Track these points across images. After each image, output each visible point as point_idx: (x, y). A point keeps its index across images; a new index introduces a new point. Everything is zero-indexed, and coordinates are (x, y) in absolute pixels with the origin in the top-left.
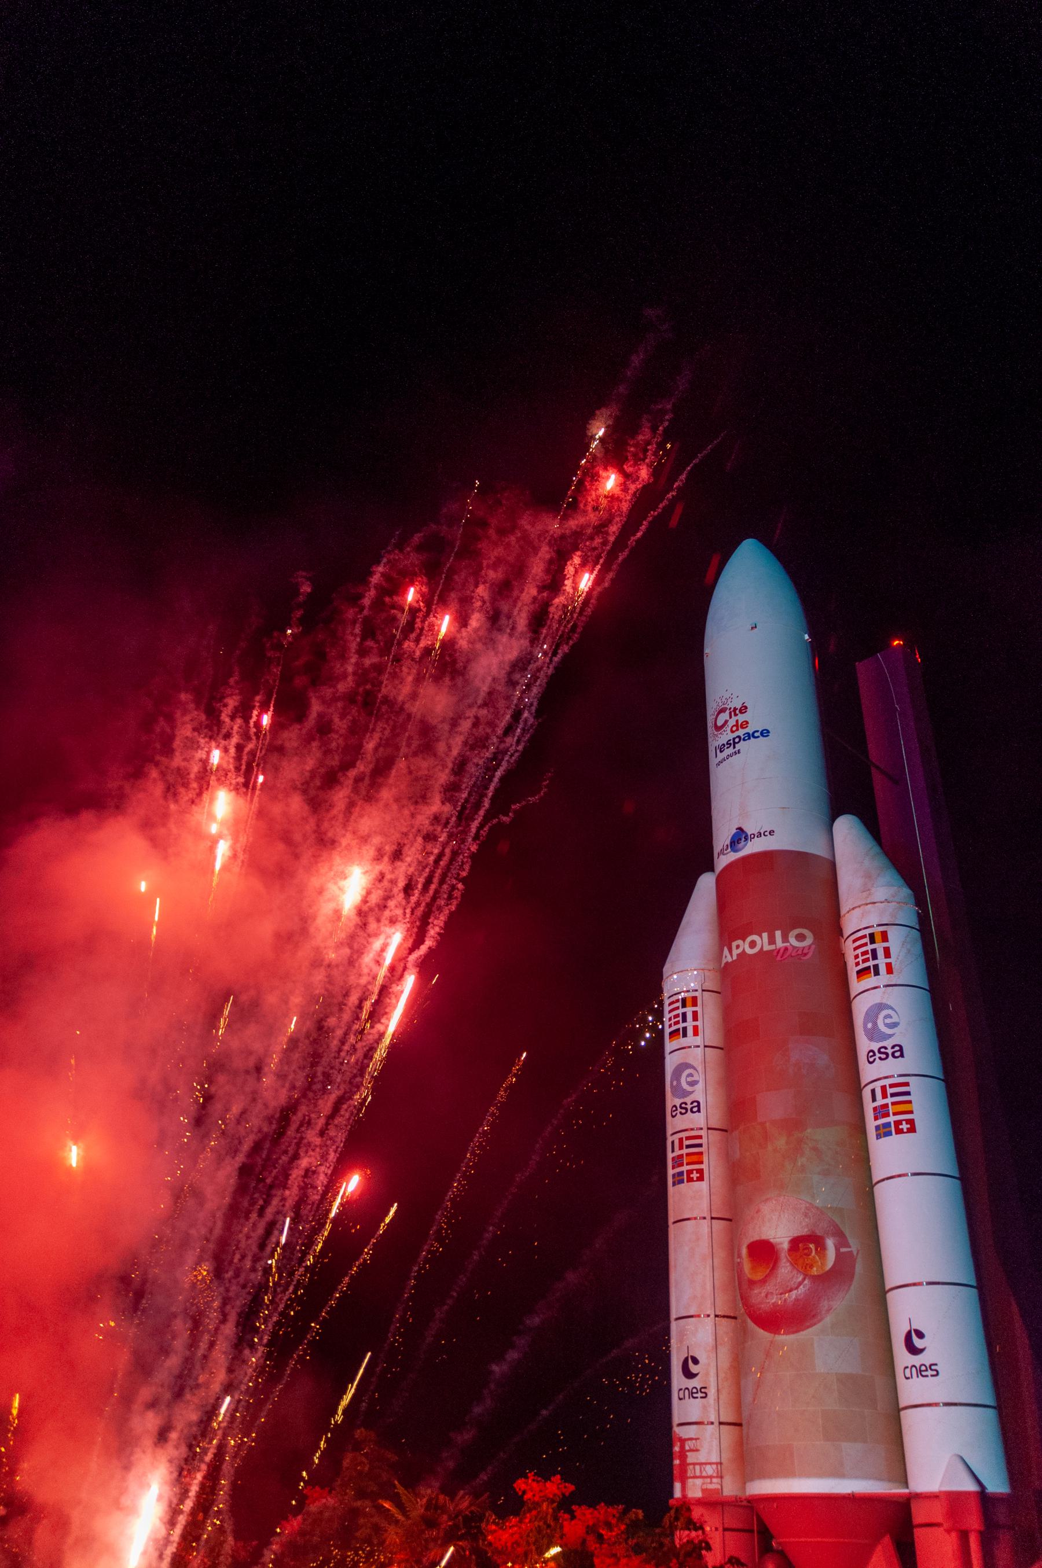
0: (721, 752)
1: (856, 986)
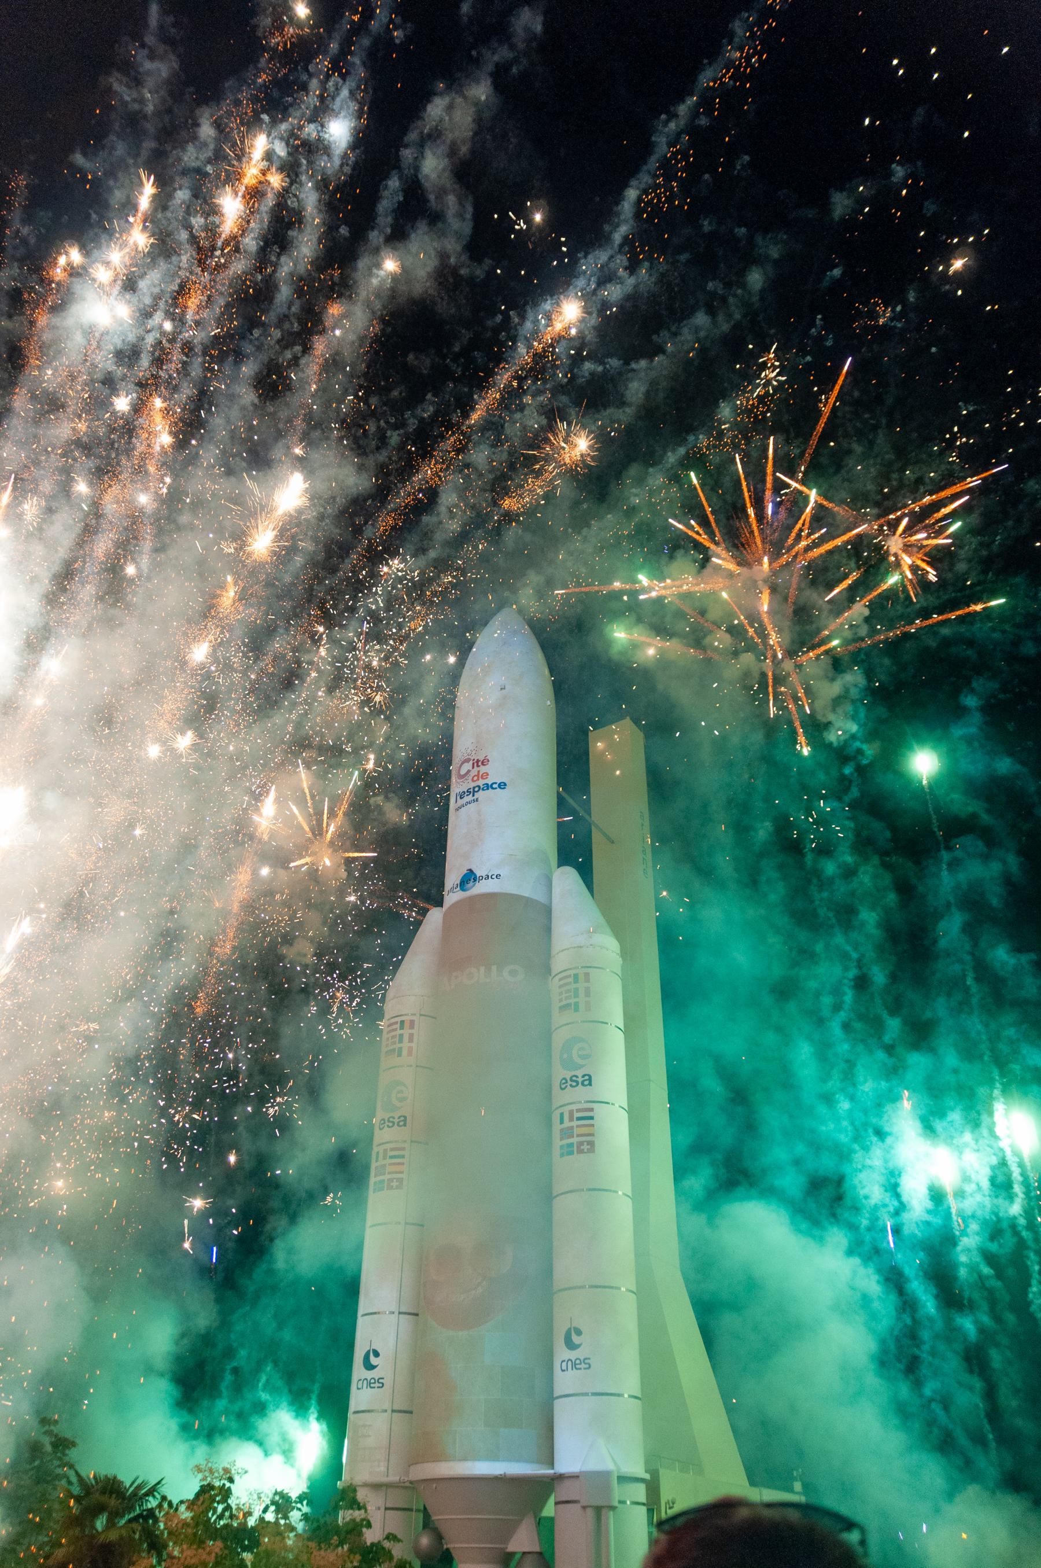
1: (558, 1019)
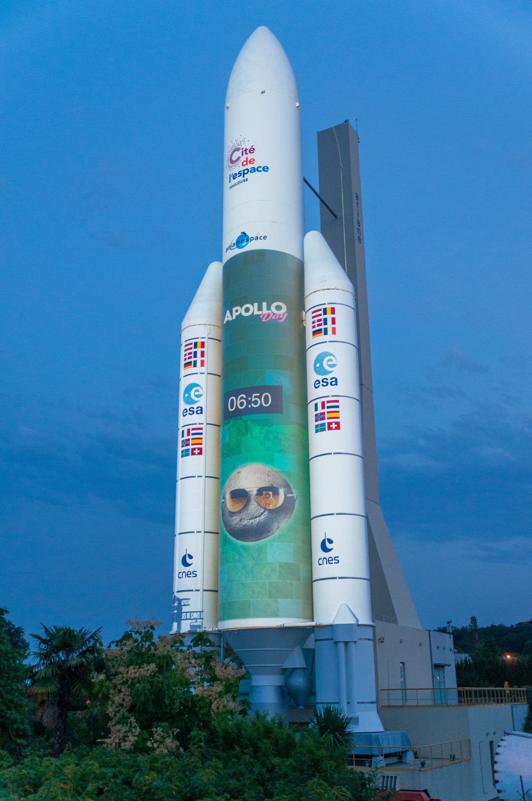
0: (234, 179)
1: (310, 340)
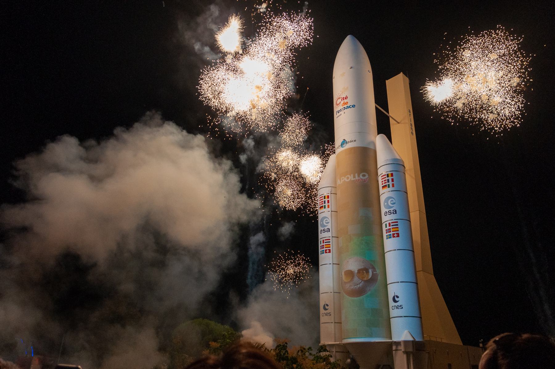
0: (338, 113)
1: (381, 191)
